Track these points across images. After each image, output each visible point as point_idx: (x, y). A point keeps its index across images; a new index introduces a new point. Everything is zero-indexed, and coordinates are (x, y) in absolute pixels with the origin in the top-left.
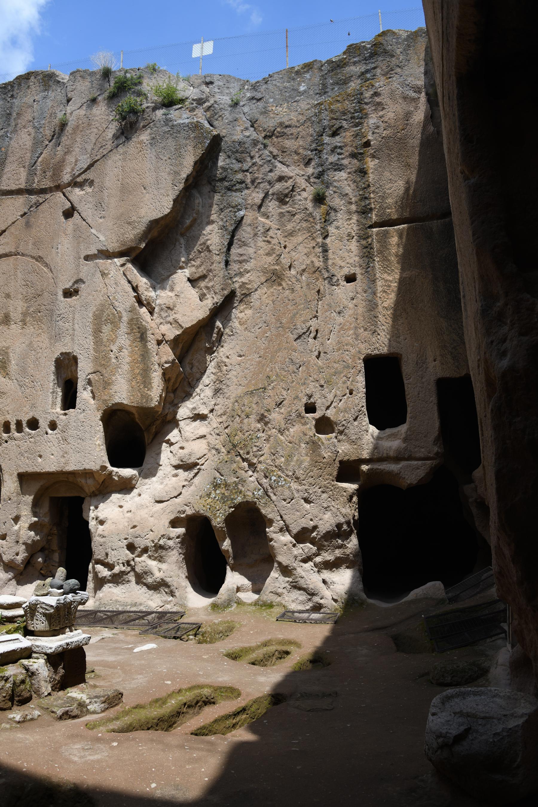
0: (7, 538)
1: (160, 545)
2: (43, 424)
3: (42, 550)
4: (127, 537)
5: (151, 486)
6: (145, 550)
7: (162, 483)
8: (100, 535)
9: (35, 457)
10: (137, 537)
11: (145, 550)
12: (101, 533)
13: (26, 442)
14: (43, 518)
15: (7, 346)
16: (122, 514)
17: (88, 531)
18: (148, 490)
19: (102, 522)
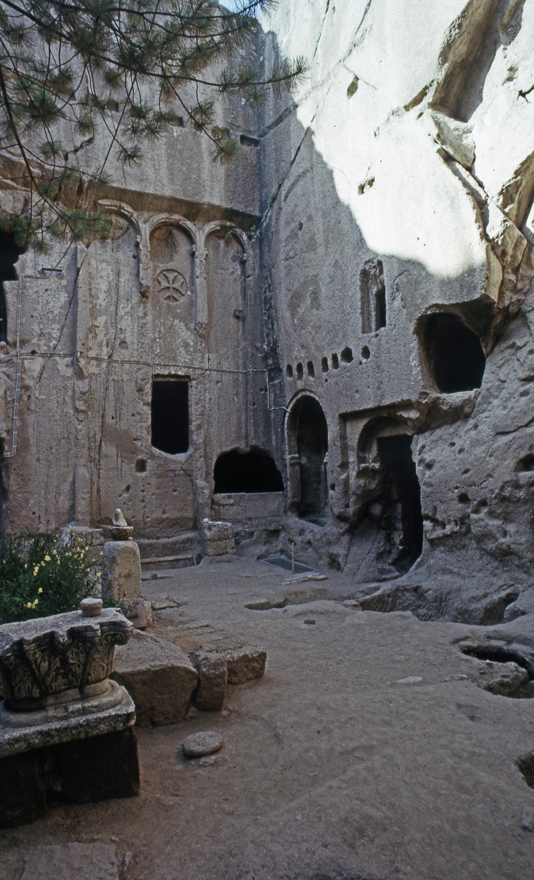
0: (336, 488)
1: (504, 496)
2: (357, 353)
3: (378, 500)
4: (459, 485)
5: (492, 413)
6: (483, 503)
7: (505, 408)
8: (426, 484)
9: (352, 393)
10: (471, 486)
11: (483, 503)
12: (428, 480)
13: (343, 377)
14: (373, 464)
15: (316, 273)
16: (453, 454)
17: (416, 478)
18: (487, 419)
19: (429, 466)
